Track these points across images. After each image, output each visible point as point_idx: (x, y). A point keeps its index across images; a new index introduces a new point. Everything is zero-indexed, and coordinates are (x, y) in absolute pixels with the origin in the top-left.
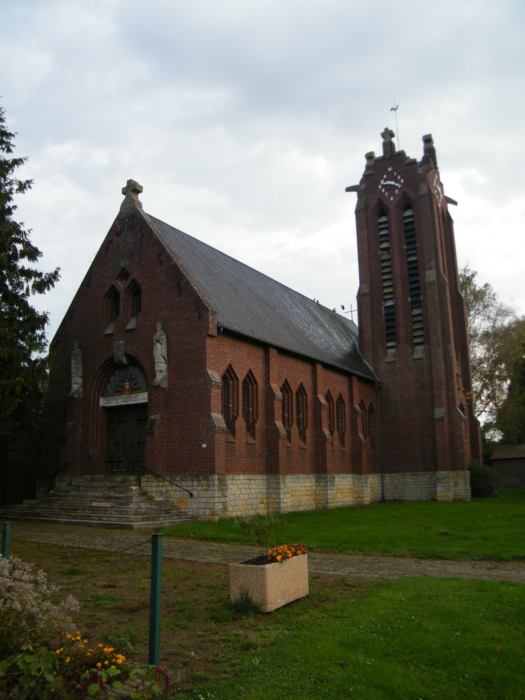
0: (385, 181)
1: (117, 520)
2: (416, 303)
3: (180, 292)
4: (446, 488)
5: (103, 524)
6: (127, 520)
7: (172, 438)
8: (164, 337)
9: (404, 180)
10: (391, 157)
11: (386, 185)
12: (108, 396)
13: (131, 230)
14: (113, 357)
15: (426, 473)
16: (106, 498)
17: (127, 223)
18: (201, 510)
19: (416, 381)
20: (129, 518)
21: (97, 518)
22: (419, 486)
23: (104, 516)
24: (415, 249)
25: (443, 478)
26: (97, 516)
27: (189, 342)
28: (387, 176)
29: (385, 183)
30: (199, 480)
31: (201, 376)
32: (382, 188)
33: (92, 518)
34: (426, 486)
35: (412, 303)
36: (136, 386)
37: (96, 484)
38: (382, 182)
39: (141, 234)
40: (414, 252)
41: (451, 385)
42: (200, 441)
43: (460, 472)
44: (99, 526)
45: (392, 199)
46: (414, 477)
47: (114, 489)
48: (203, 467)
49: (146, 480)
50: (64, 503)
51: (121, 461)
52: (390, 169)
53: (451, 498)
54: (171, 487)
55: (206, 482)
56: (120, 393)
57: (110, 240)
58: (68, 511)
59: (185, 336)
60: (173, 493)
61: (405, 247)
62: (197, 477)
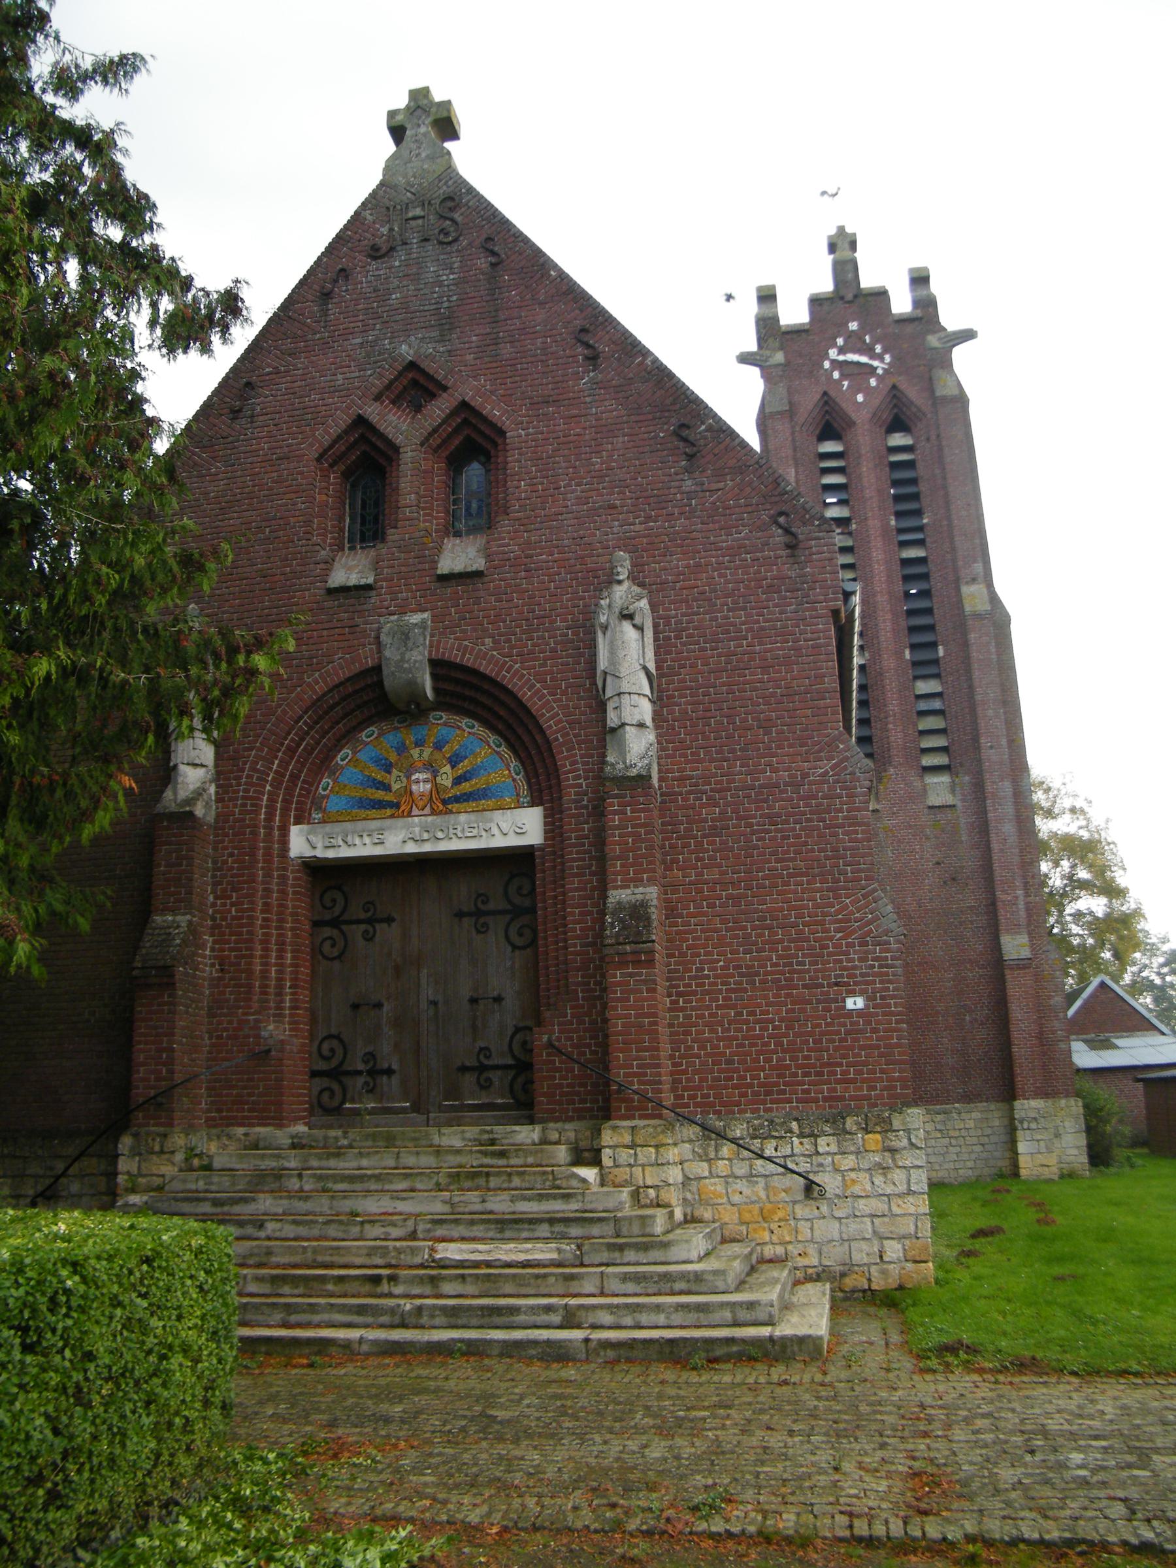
0: (842, 351)
1: (677, 1318)
2: (926, 666)
3: (690, 457)
4: (1042, 1143)
5: (632, 1344)
6: (743, 1315)
7: (696, 977)
8: (644, 603)
9: (892, 357)
10: (856, 296)
11: (846, 362)
12: (323, 822)
13: (441, 243)
14: (378, 669)
15: (972, 1105)
16: (497, 1221)
17: (420, 222)
18: (864, 1246)
19: (938, 863)
20: (751, 1305)
21: (556, 1318)
22: (954, 1142)
23: (594, 1307)
24: (920, 529)
25: (1035, 1119)
26: (548, 1309)
27: (751, 630)
28: (845, 341)
29: (841, 358)
30: (842, 1133)
31: (820, 751)
32: (833, 368)
33: (522, 1318)
34: (975, 1140)
35: (915, 664)
36: (466, 787)
37: (354, 1164)
38: (833, 353)
39: (493, 260)
40: (920, 536)
41: (1033, 877)
42: (829, 985)
43: (1063, 1102)
44: (611, 1354)
45: (860, 398)
46: (939, 1118)
47: (481, 1181)
48: (853, 1081)
49: (627, 1139)
50: (269, 1253)
51: (389, 1072)
52: (853, 326)
53: (1055, 1170)
54: (705, 1165)
55: (878, 1137)
56: (389, 812)
57: (343, 270)
58: (330, 1287)
59: (729, 610)
60: (720, 1188)
61: (893, 523)
62: (836, 1120)
